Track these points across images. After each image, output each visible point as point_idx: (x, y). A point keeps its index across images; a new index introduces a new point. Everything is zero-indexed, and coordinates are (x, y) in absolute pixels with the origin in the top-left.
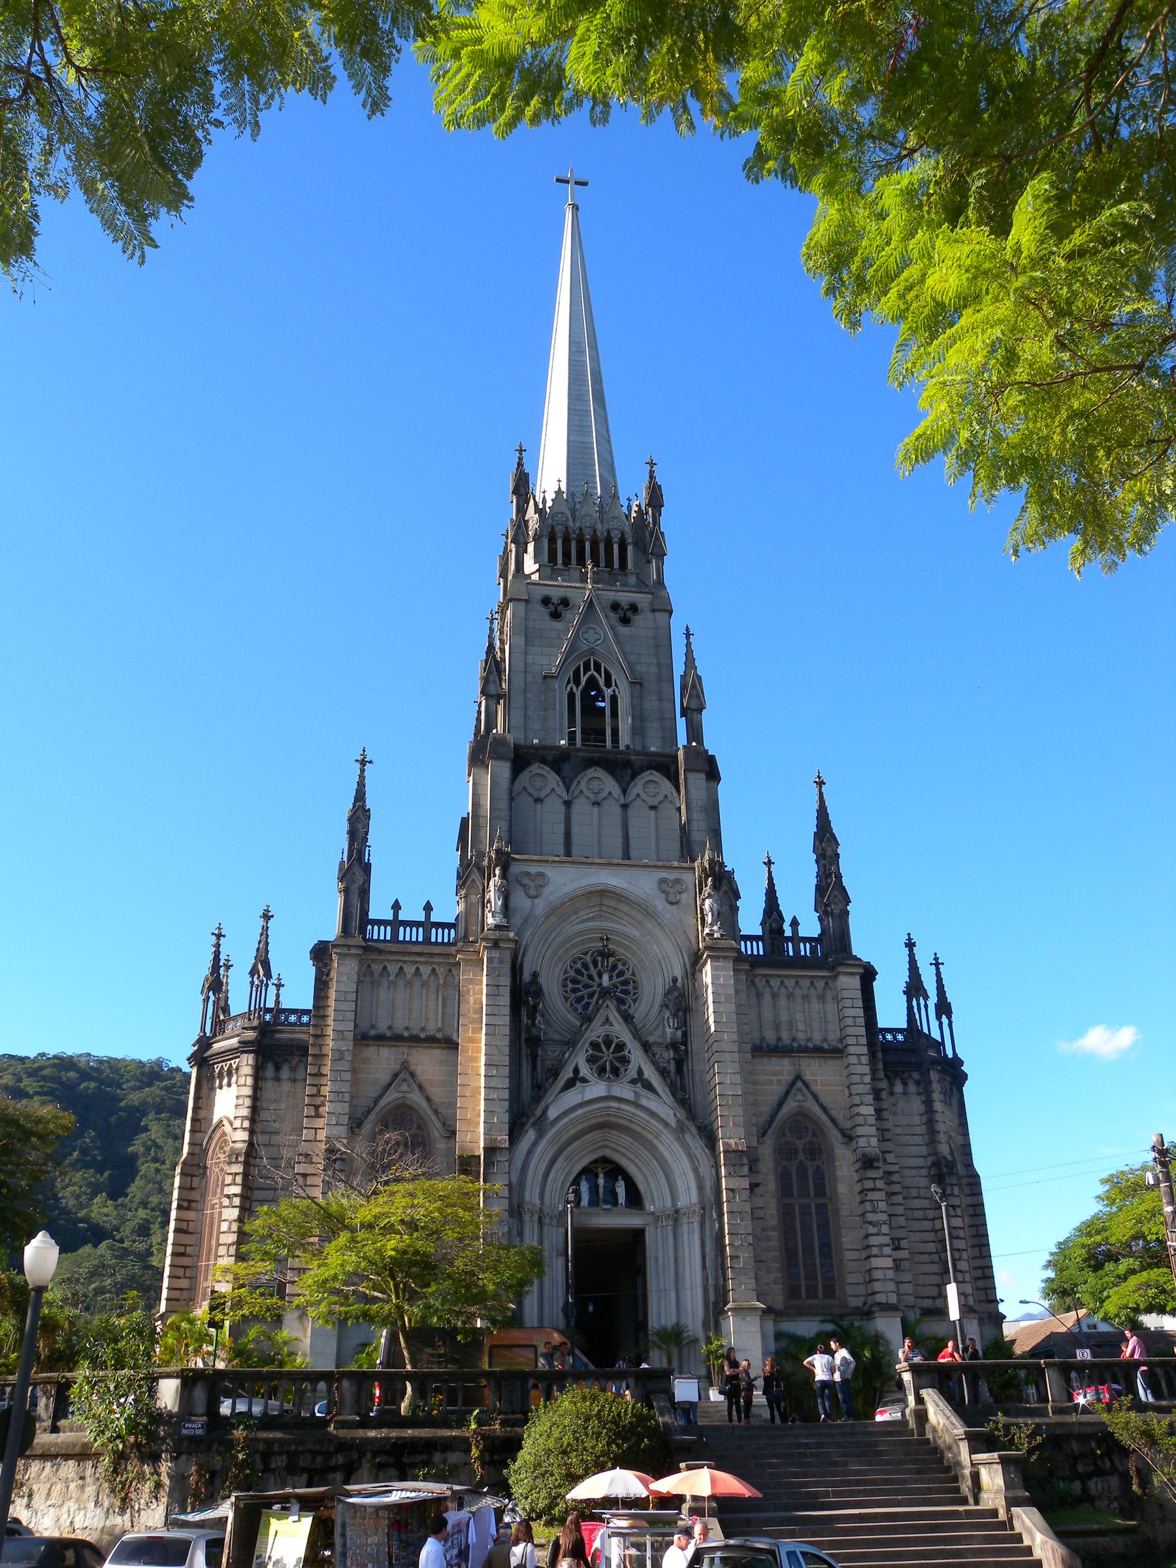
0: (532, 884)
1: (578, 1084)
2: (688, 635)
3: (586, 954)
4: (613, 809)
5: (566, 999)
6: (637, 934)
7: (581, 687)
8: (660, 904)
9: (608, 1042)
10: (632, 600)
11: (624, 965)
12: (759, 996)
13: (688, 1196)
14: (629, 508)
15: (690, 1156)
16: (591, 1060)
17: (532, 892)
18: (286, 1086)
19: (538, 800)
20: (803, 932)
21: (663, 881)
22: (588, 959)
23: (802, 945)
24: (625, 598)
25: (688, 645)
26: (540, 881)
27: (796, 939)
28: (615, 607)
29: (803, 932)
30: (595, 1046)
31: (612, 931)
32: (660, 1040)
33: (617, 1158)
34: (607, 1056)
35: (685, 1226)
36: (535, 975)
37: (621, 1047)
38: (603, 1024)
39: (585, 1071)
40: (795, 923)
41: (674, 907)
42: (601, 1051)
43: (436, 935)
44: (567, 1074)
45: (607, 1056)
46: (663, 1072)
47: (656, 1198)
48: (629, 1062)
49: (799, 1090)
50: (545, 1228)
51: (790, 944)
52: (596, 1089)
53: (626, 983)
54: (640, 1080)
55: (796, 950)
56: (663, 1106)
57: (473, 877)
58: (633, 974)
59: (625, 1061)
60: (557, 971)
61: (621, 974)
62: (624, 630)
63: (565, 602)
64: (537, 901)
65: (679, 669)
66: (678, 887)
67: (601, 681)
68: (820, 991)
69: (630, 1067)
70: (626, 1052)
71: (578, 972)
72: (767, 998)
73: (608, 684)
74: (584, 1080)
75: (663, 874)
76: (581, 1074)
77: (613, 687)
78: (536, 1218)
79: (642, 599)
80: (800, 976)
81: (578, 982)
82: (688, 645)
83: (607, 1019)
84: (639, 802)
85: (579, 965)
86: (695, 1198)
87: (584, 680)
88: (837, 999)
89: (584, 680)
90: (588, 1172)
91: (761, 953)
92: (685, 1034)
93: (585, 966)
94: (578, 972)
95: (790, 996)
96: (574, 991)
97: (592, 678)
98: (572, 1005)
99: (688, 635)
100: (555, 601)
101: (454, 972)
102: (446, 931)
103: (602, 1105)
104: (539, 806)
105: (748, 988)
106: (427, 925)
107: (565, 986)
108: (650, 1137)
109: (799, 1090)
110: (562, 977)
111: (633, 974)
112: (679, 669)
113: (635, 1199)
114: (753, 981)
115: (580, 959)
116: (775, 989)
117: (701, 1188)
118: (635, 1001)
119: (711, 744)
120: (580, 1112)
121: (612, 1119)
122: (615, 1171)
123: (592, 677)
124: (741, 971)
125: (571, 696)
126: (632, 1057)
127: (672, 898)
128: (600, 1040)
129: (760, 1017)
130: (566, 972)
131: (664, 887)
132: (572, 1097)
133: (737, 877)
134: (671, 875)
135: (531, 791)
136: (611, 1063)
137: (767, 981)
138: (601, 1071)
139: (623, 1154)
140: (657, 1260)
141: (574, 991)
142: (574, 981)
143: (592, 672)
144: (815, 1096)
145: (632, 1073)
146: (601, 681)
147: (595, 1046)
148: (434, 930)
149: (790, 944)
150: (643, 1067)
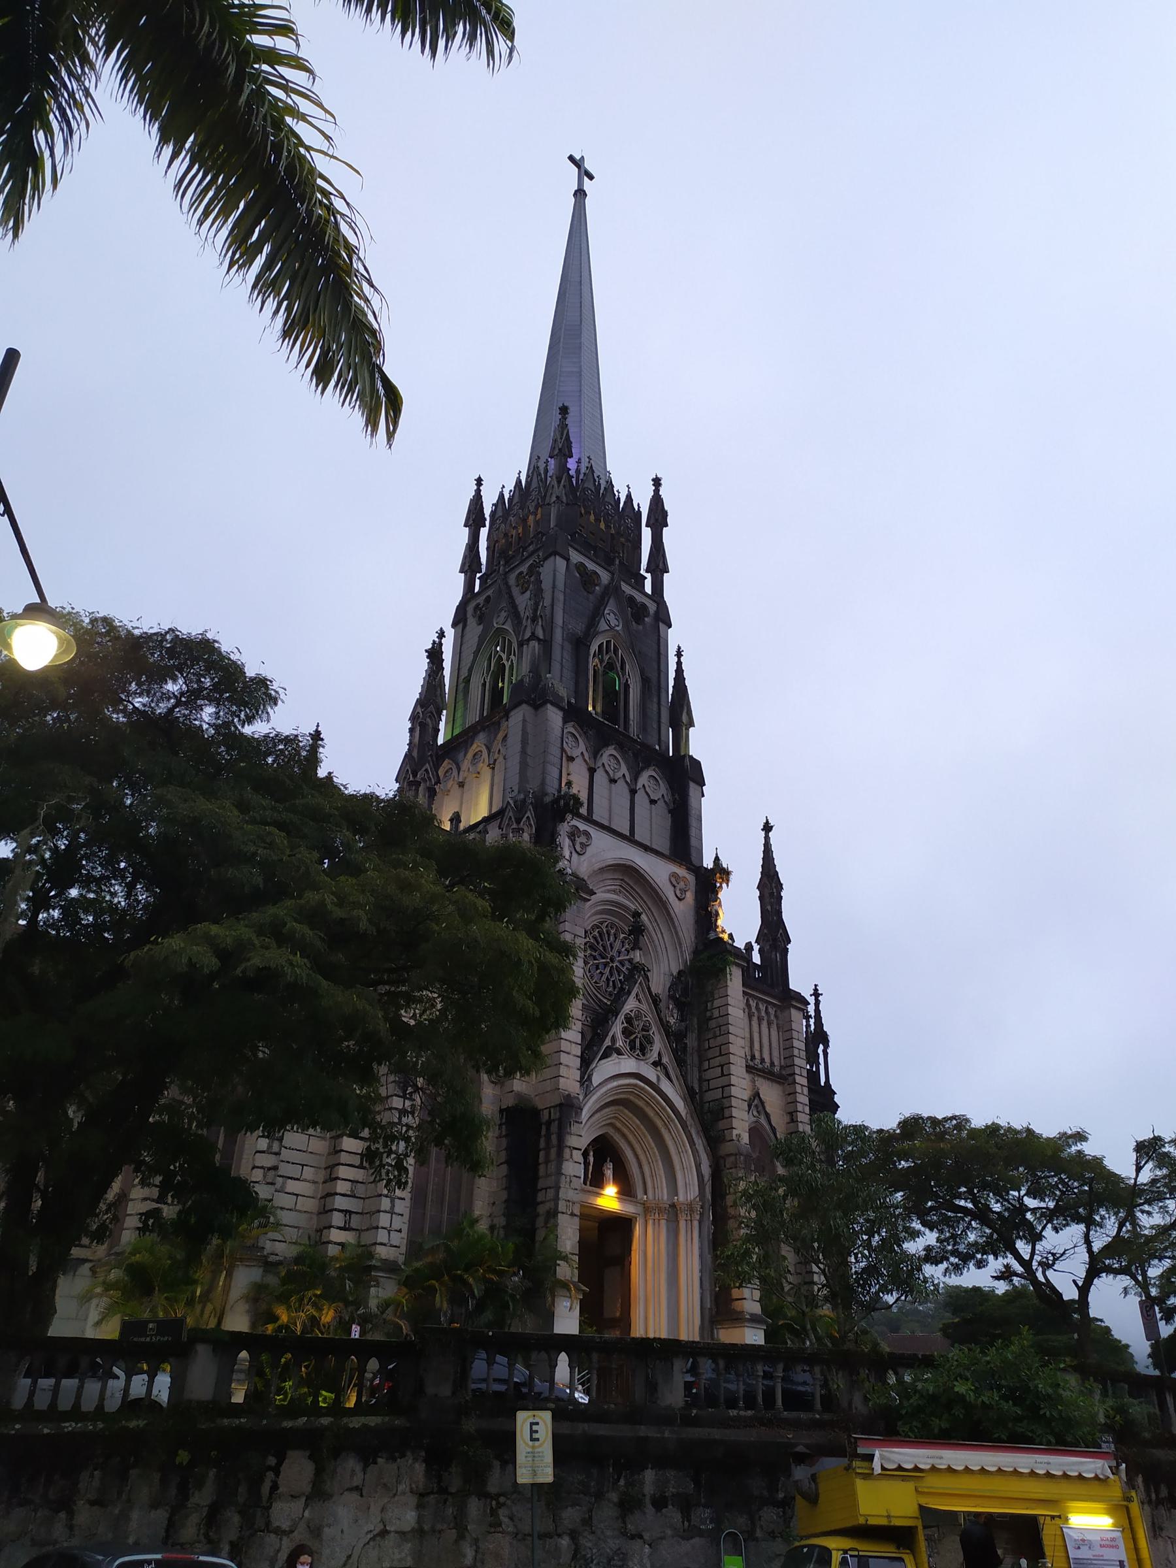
2: (679, 654)
4: (621, 789)
8: (669, 894)
15: (695, 1152)
16: (626, 1033)
21: (674, 875)
30: (628, 1019)
33: (617, 1137)
39: (620, 1043)
44: (608, 1042)
57: (528, 814)
64: (583, 858)
74: (619, 1053)
99: (679, 654)
108: (659, 1123)
112: (671, 683)
120: (615, 1084)
121: (632, 1098)
139: (624, 1136)
144: (767, 1116)
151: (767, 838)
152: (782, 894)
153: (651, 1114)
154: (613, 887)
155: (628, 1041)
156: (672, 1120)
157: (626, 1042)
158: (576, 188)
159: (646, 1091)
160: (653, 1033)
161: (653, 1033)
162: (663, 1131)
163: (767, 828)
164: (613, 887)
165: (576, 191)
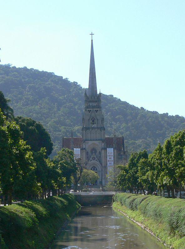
9: (94, 157)
13: (100, 170)
45: (94, 158)
46: (98, 159)
47: (98, 170)
52: (93, 161)
54: (96, 160)
56: (98, 162)
62: (96, 113)
75: (99, 141)
79: (98, 109)
90: (93, 167)
113: (97, 170)
122: (95, 167)
132: (91, 162)
134: (100, 141)
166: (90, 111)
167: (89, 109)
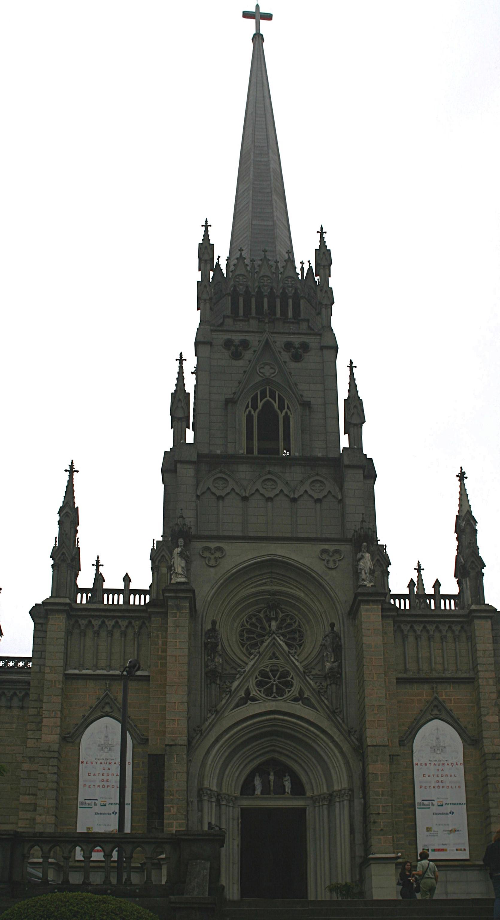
0: (212, 557)
1: (249, 702)
2: (351, 367)
3: (259, 612)
5: (243, 645)
6: (301, 595)
7: (257, 411)
10: (302, 340)
11: (291, 619)
12: (404, 638)
14: (302, 269)
16: (259, 684)
17: (212, 563)
18: (16, 712)
19: (220, 498)
20: (443, 591)
21: (324, 551)
22: (262, 615)
23: (442, 601)
24: (296, 340)
25: (352, 375)
26: (218, 554)
27: (437, 596)
28: (288, 346)
29: (443, 591)
31: (281, 593)
32: (319, 673)
34: (274, 681)
35: (337, 804)
36: (214, 623)
37: (285, 674)
38: (271, 658)
40: (437, 585)
41: (333, 572)
42: (270, 678)
43: (134, 600)
45: (274, 681)
48: (292, 685)
49: (436, 706)
50: (223, 807)
51: (432, 601)
53: (293, 632)
54: (299, 698)
55: (438, 605)
58: (299, 625)
59: (289, 685)
60: (236, 625)
61: (290, 625)
63: (245, 344)
65: (343, 393)
66: (337, 557)
67: (276, 406)
68: (457, 633)
69: (293, 689)
70: (289, 679)
71: (252, 624)
72: (411, 639)
73: (282, 407)
74: (254, 699)
76: (251, 695)
77: (286, 409)
78: (214, 799)
79: (313, 342)
80: (440, 622)
81: (253, 633)
82: (352, 375)
83: (274, 654)
84: (306, 497)
85: (254, 620)
86: (345, 785)
87: (260, 405)
88: (471, 639)
89: (260, 405)
91: (408, 607)
92: (340, 666)
93: (259, 620)
94: (252, 624)
95: (430, 638)
96: (249, 639)
97: (268, 403)
98: (247, 649)
99: (351, 367)
100: (237, 343)
101: (147, 624)
102: (142, 596)
103: (268, 717)
104: (221, 502)
105: (395, 631)
106: (127, 592)
107: (241, 635)
108: (310, 742)
109: (436, 706)
110: (239, 629)
111: (299, 625)
112: (343, 393)
114: (399, 627)
115: (255, 615)
116: (419, 633)
117: (350, 777)
118: (300, 646)
119: (368, 450)
123: (268, 403)
124: (388, 617)
125: (250, 418)
126: (295, 682)
127: (331, 565)
128: (268, 670)
129: (404, 653)
130: (243, 625)
131: (325, 556)
133: (389, 551)
134: (331, 547)
135: (213, 490)
136: (276, 685)
137: (412, 627)
138: (269, 692)
140: (314, 829)
141: (249, 639)
142: (249, 631)
143: (268, 398)
145: (294, 691)
146: (276, 406)
147: (263, 674)
148: (132, 596)
149: (432, 601)
150: (303, 687)
151: (463, 487)
152: (477, 527)
153: (300, 736)
154: (264, 581)
155: (287, 690)
156: (318, 736)
157: (260, 691)
158: (255, 32)
159: (287, 721)
160: (292, 678)
161: (292, 678)
162: (313, 744)
163: (462, 476)
164: (264, 581)
165: (254, 35)
166: (245, 344)
167: (237, 338)
